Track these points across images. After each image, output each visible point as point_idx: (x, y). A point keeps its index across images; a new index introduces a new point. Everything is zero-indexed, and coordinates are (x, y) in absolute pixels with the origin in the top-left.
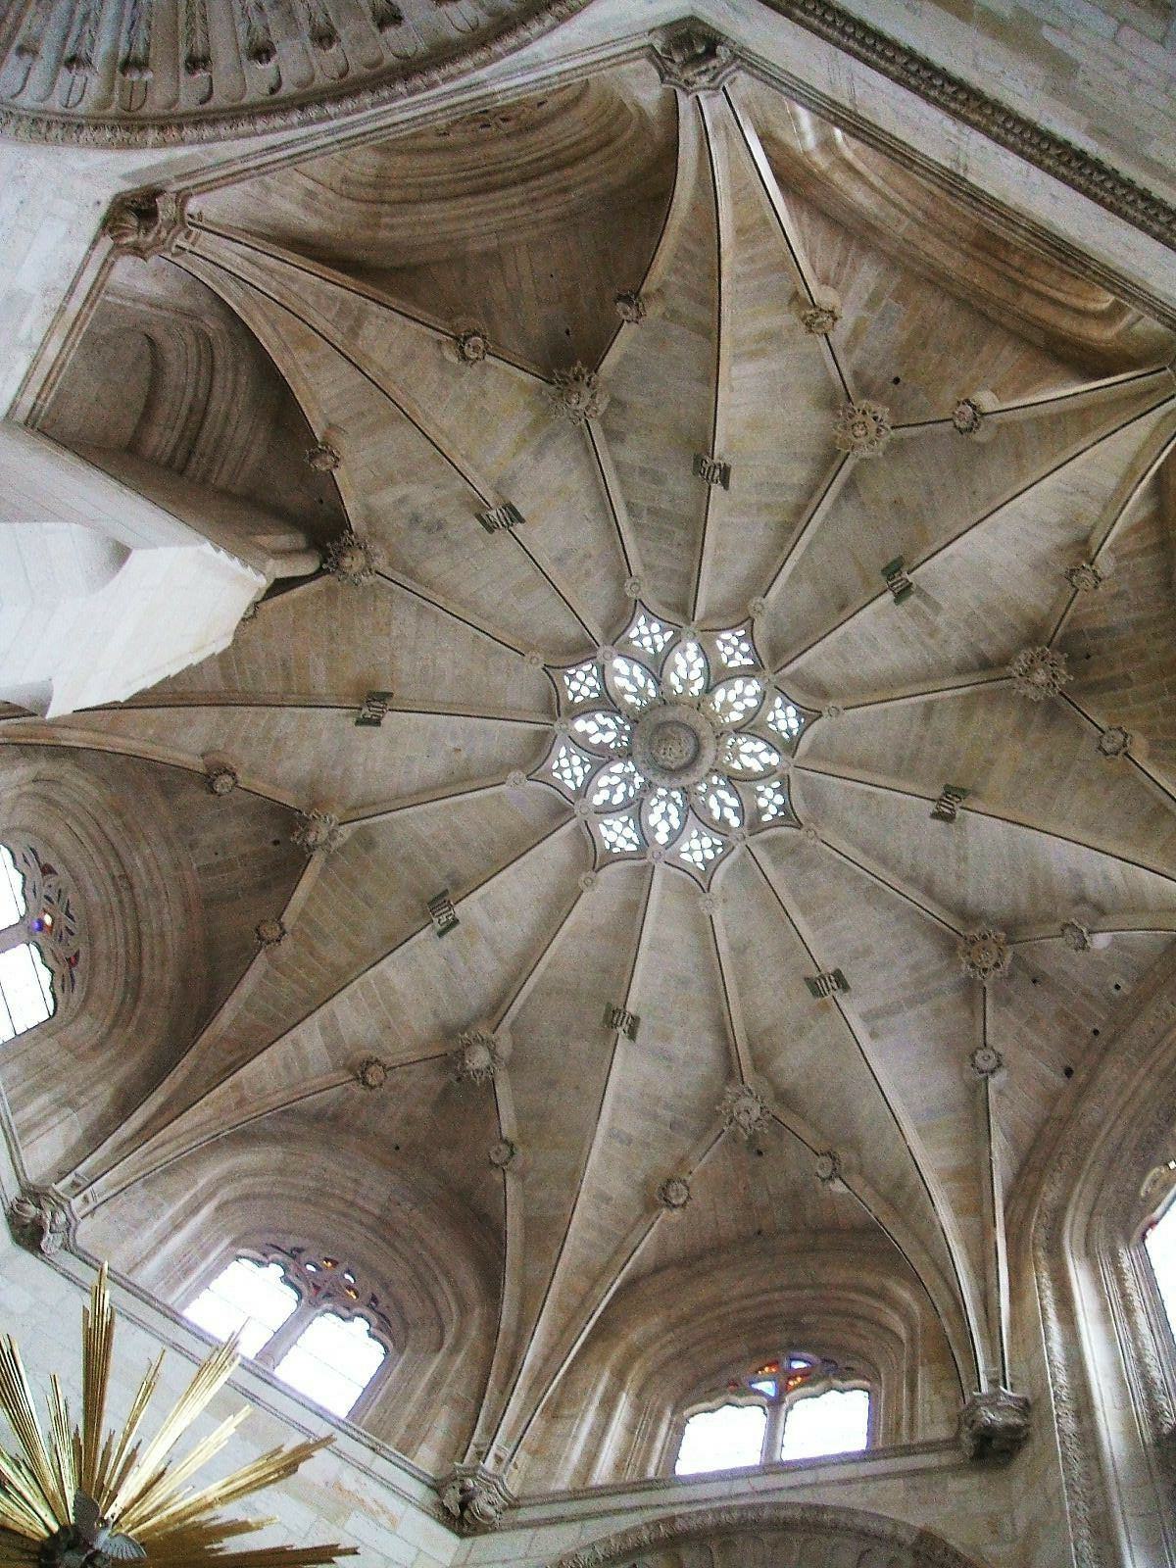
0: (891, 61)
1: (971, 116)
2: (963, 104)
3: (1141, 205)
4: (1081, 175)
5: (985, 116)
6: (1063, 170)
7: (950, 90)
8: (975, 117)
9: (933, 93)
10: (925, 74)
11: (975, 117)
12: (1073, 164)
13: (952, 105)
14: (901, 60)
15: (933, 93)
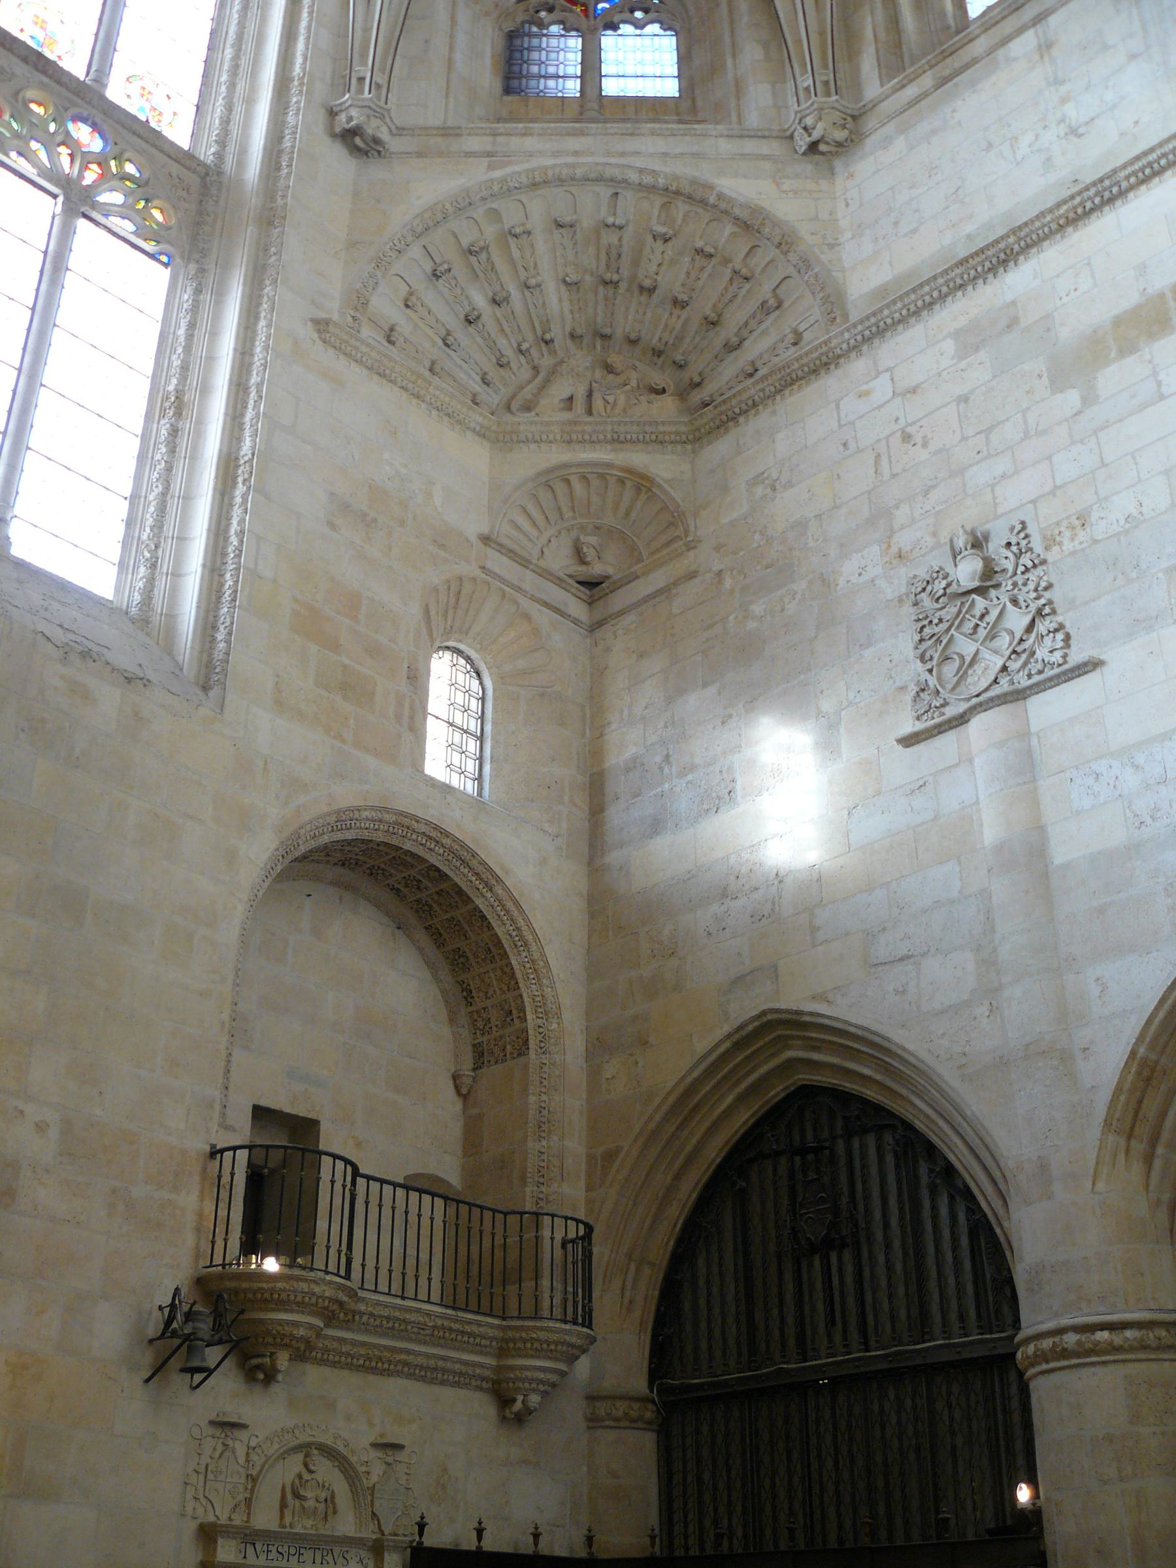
0: (1127, 178)
1: (1065, 207)
2: (1075, 208)
3: (959, 281)
4: (994, 256)
5: (1060, 217)
6: (1002, 245)
7: (1089, 205)
8: (1062, 211)
9: (1092, 191)
10: (1107, 195)
11: (1062, 211)
12: (1002, 256)
13: (1078, 199)
14: (1124, 185)
15: (1092, 191)
